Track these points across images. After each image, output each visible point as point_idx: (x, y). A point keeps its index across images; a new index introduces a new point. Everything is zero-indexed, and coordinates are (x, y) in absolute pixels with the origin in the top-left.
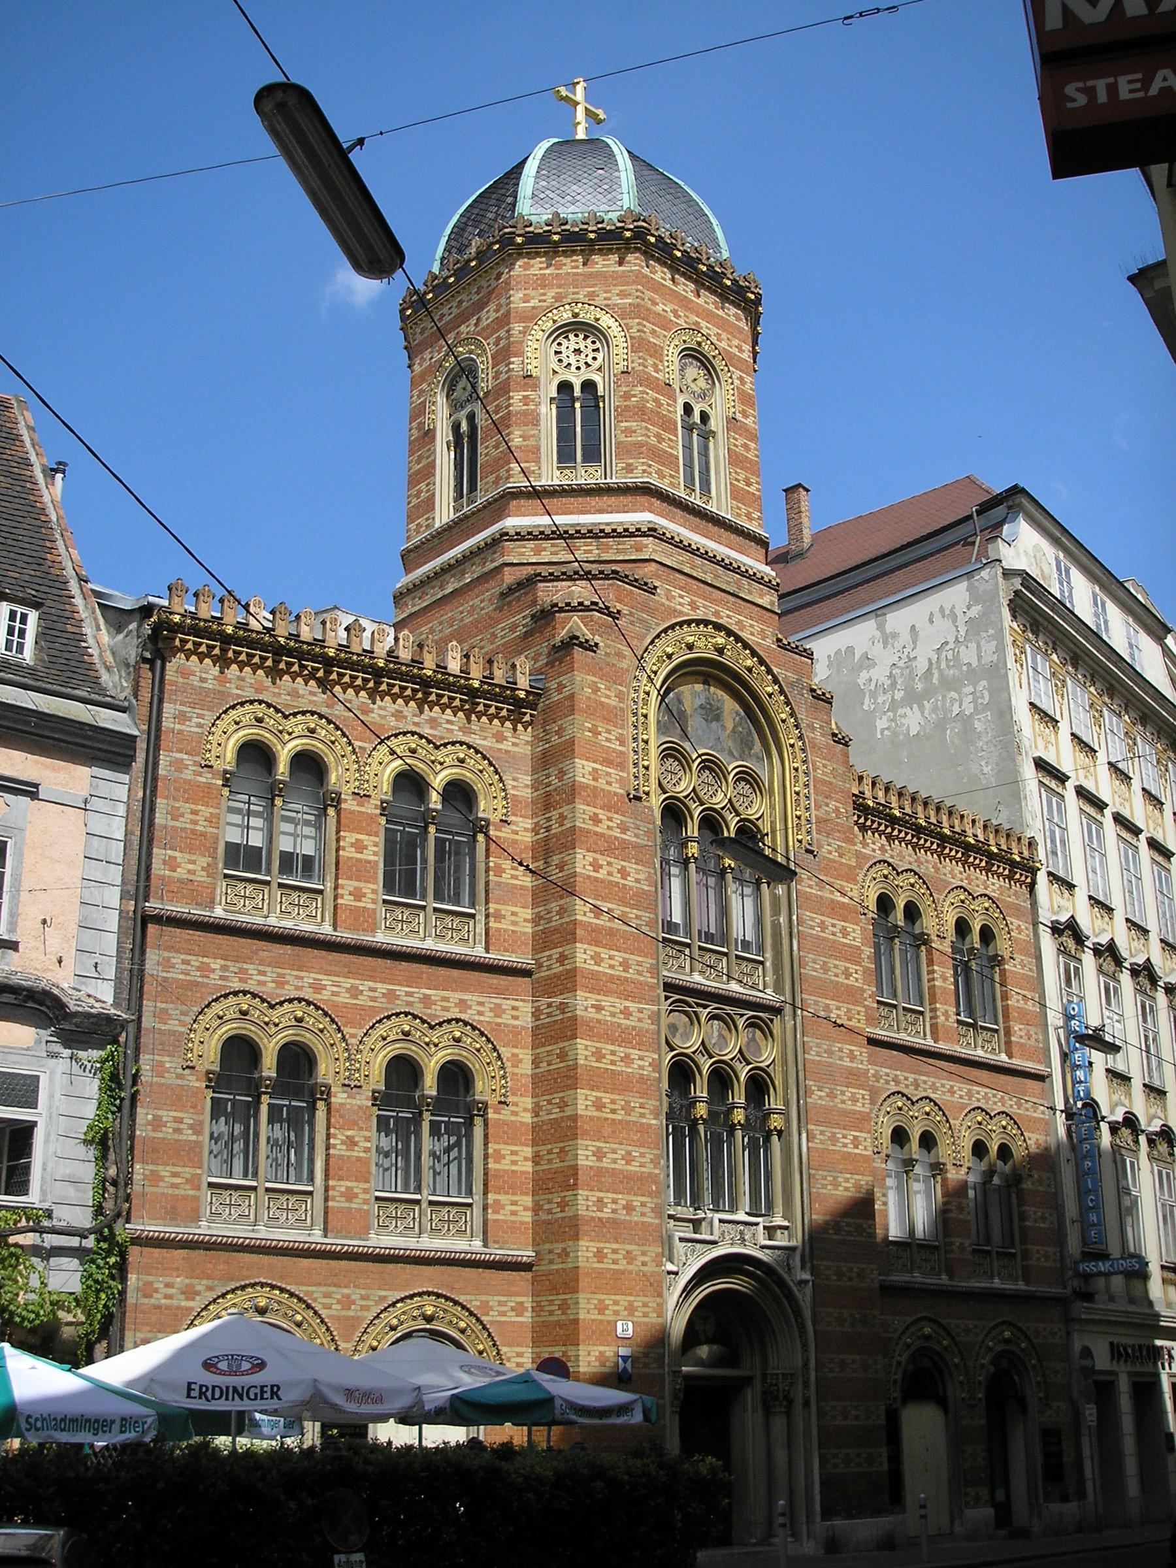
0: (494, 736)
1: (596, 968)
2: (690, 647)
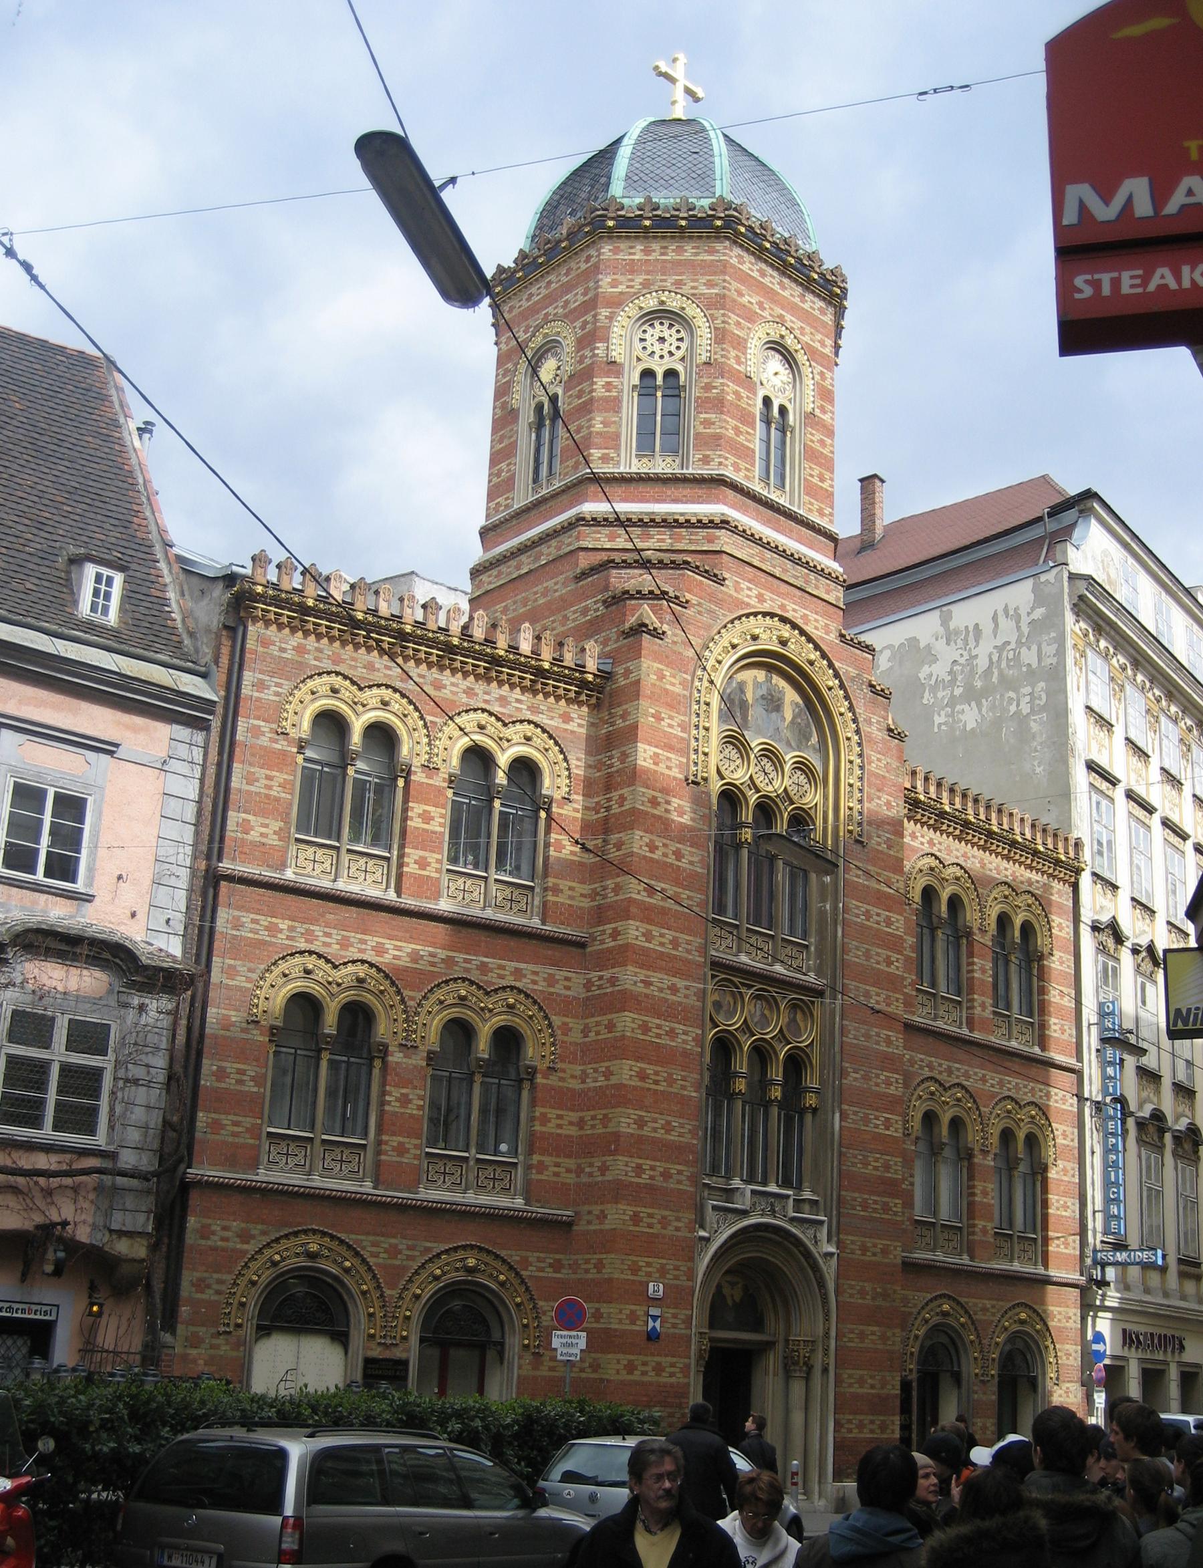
0: (561, 716)
1: (647, 945)
2: (755, 638)
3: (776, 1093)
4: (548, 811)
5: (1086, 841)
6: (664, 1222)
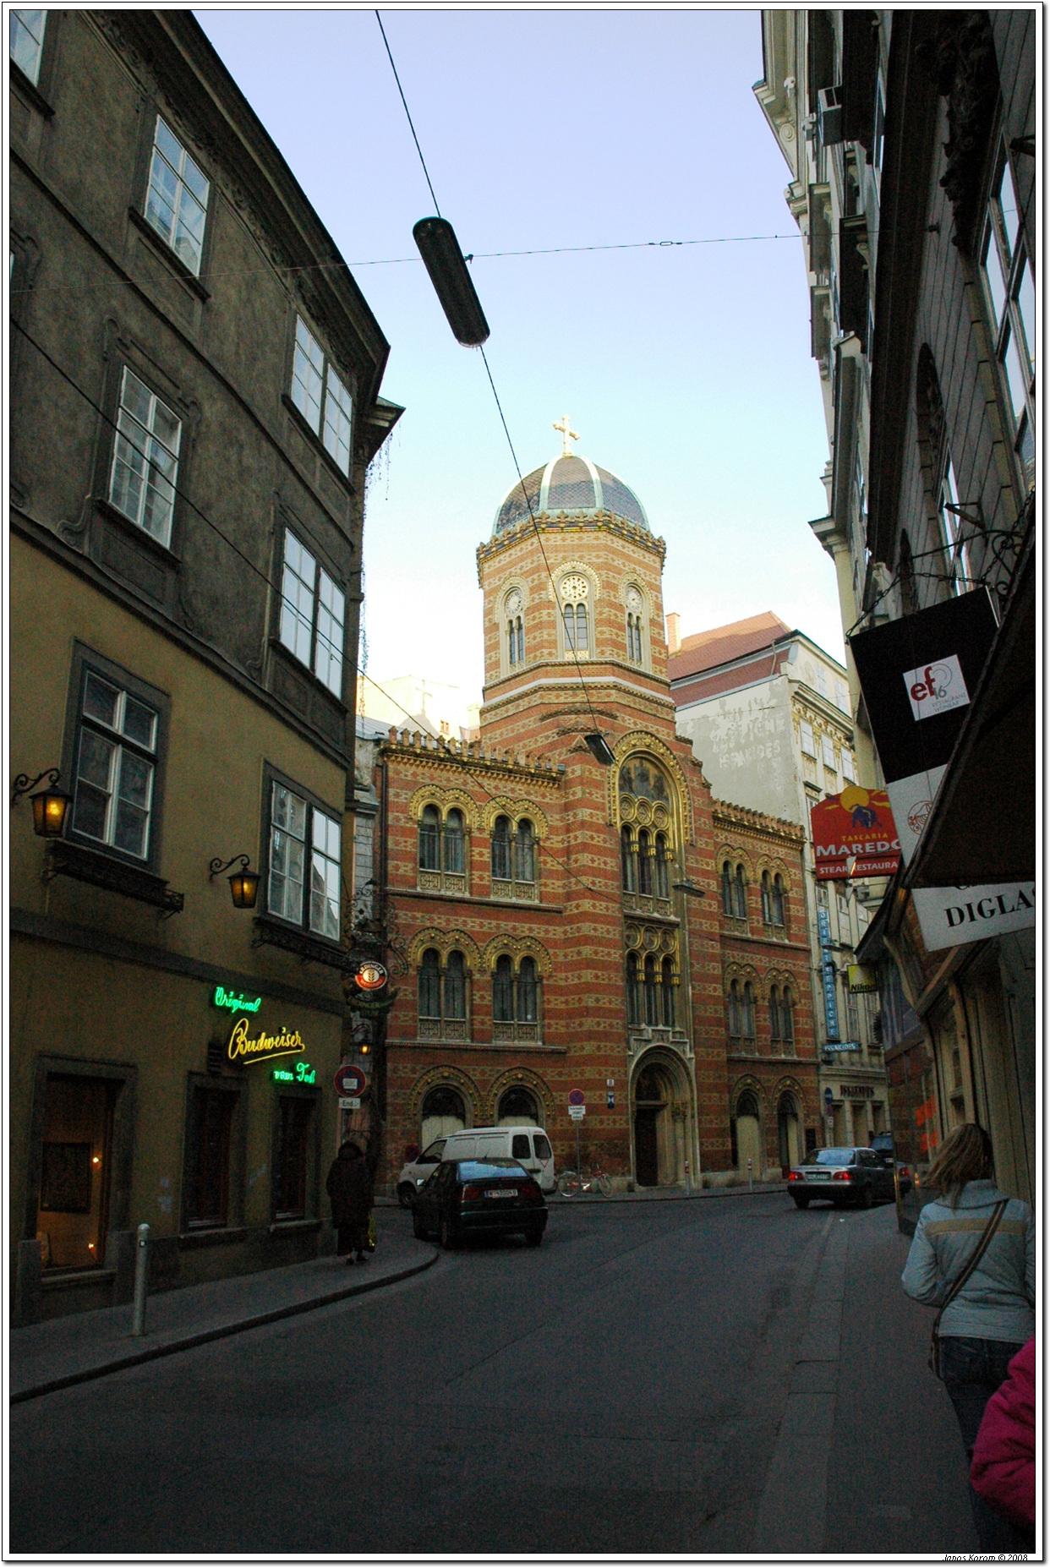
2: (634, 746)
3: (659, 979)
4: (538, 844)
5: (806, 826)
6: (612, 1049)
